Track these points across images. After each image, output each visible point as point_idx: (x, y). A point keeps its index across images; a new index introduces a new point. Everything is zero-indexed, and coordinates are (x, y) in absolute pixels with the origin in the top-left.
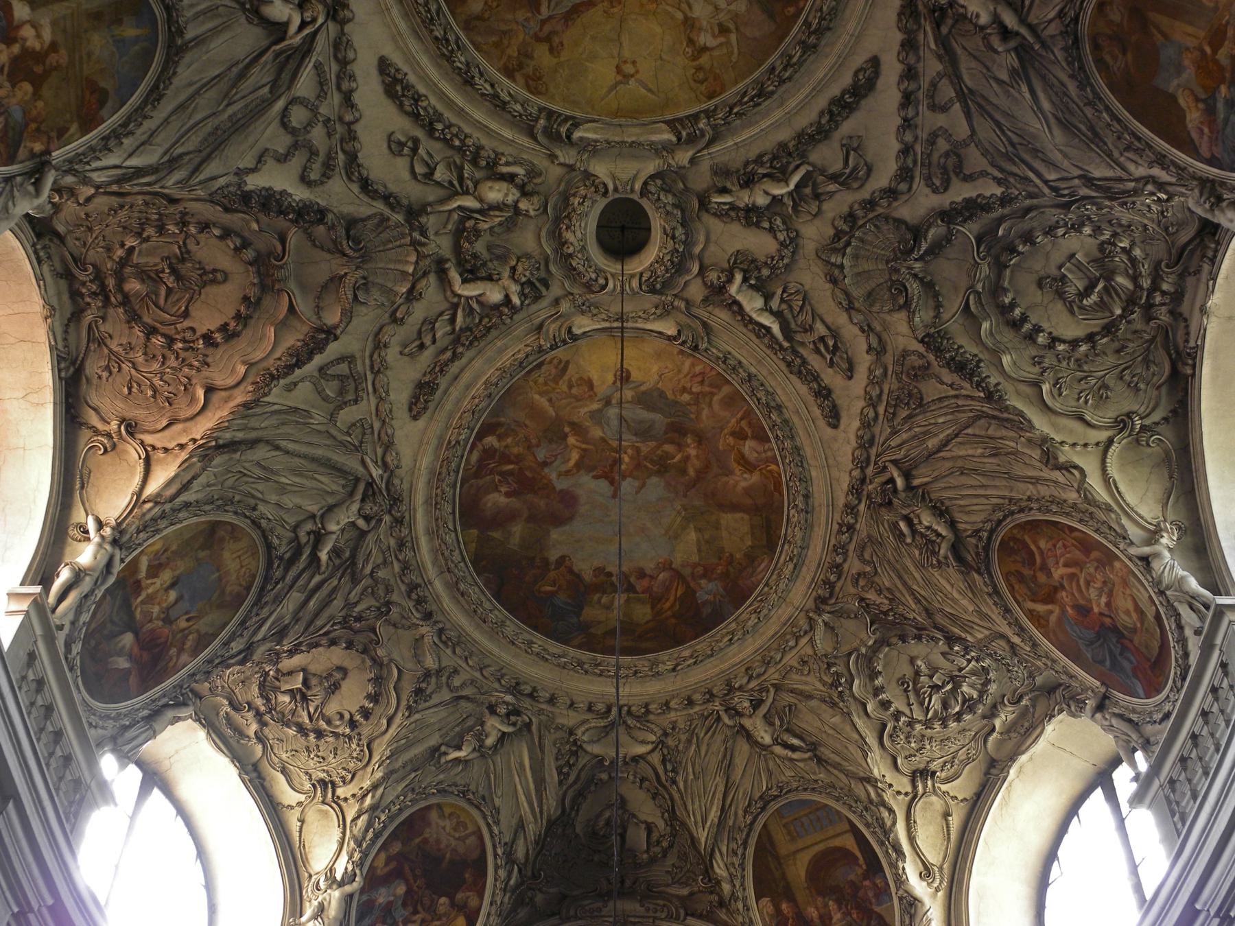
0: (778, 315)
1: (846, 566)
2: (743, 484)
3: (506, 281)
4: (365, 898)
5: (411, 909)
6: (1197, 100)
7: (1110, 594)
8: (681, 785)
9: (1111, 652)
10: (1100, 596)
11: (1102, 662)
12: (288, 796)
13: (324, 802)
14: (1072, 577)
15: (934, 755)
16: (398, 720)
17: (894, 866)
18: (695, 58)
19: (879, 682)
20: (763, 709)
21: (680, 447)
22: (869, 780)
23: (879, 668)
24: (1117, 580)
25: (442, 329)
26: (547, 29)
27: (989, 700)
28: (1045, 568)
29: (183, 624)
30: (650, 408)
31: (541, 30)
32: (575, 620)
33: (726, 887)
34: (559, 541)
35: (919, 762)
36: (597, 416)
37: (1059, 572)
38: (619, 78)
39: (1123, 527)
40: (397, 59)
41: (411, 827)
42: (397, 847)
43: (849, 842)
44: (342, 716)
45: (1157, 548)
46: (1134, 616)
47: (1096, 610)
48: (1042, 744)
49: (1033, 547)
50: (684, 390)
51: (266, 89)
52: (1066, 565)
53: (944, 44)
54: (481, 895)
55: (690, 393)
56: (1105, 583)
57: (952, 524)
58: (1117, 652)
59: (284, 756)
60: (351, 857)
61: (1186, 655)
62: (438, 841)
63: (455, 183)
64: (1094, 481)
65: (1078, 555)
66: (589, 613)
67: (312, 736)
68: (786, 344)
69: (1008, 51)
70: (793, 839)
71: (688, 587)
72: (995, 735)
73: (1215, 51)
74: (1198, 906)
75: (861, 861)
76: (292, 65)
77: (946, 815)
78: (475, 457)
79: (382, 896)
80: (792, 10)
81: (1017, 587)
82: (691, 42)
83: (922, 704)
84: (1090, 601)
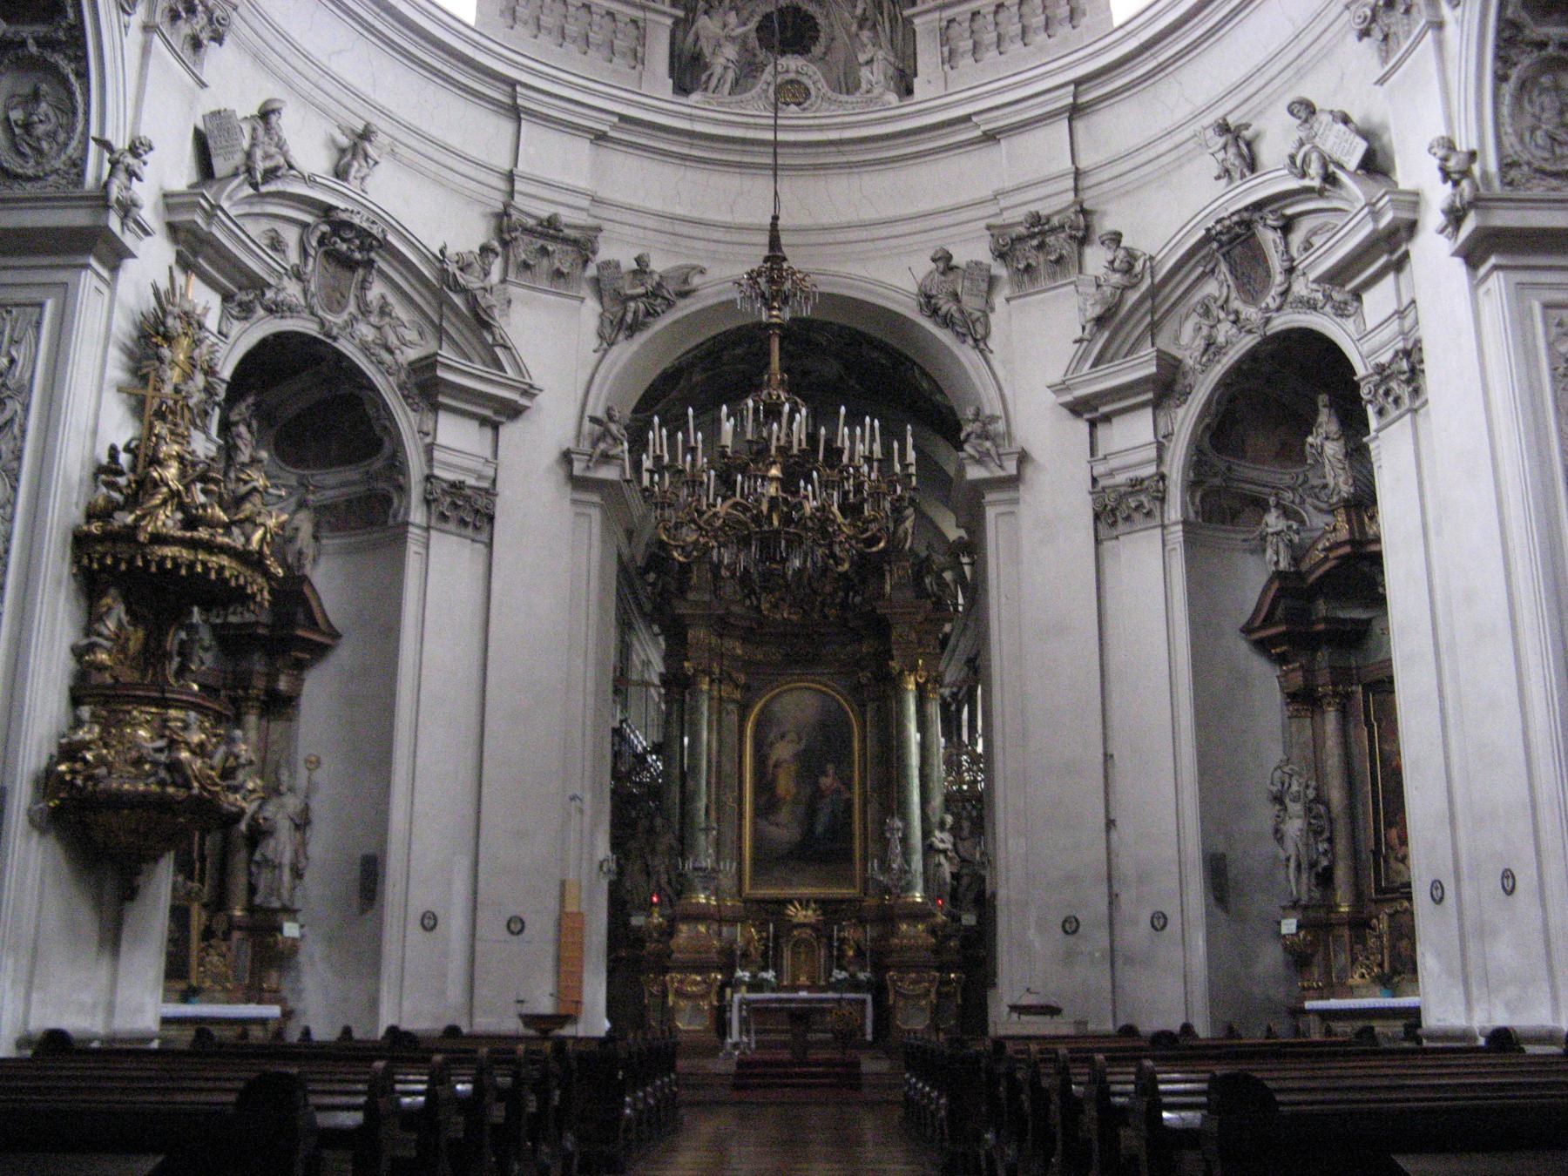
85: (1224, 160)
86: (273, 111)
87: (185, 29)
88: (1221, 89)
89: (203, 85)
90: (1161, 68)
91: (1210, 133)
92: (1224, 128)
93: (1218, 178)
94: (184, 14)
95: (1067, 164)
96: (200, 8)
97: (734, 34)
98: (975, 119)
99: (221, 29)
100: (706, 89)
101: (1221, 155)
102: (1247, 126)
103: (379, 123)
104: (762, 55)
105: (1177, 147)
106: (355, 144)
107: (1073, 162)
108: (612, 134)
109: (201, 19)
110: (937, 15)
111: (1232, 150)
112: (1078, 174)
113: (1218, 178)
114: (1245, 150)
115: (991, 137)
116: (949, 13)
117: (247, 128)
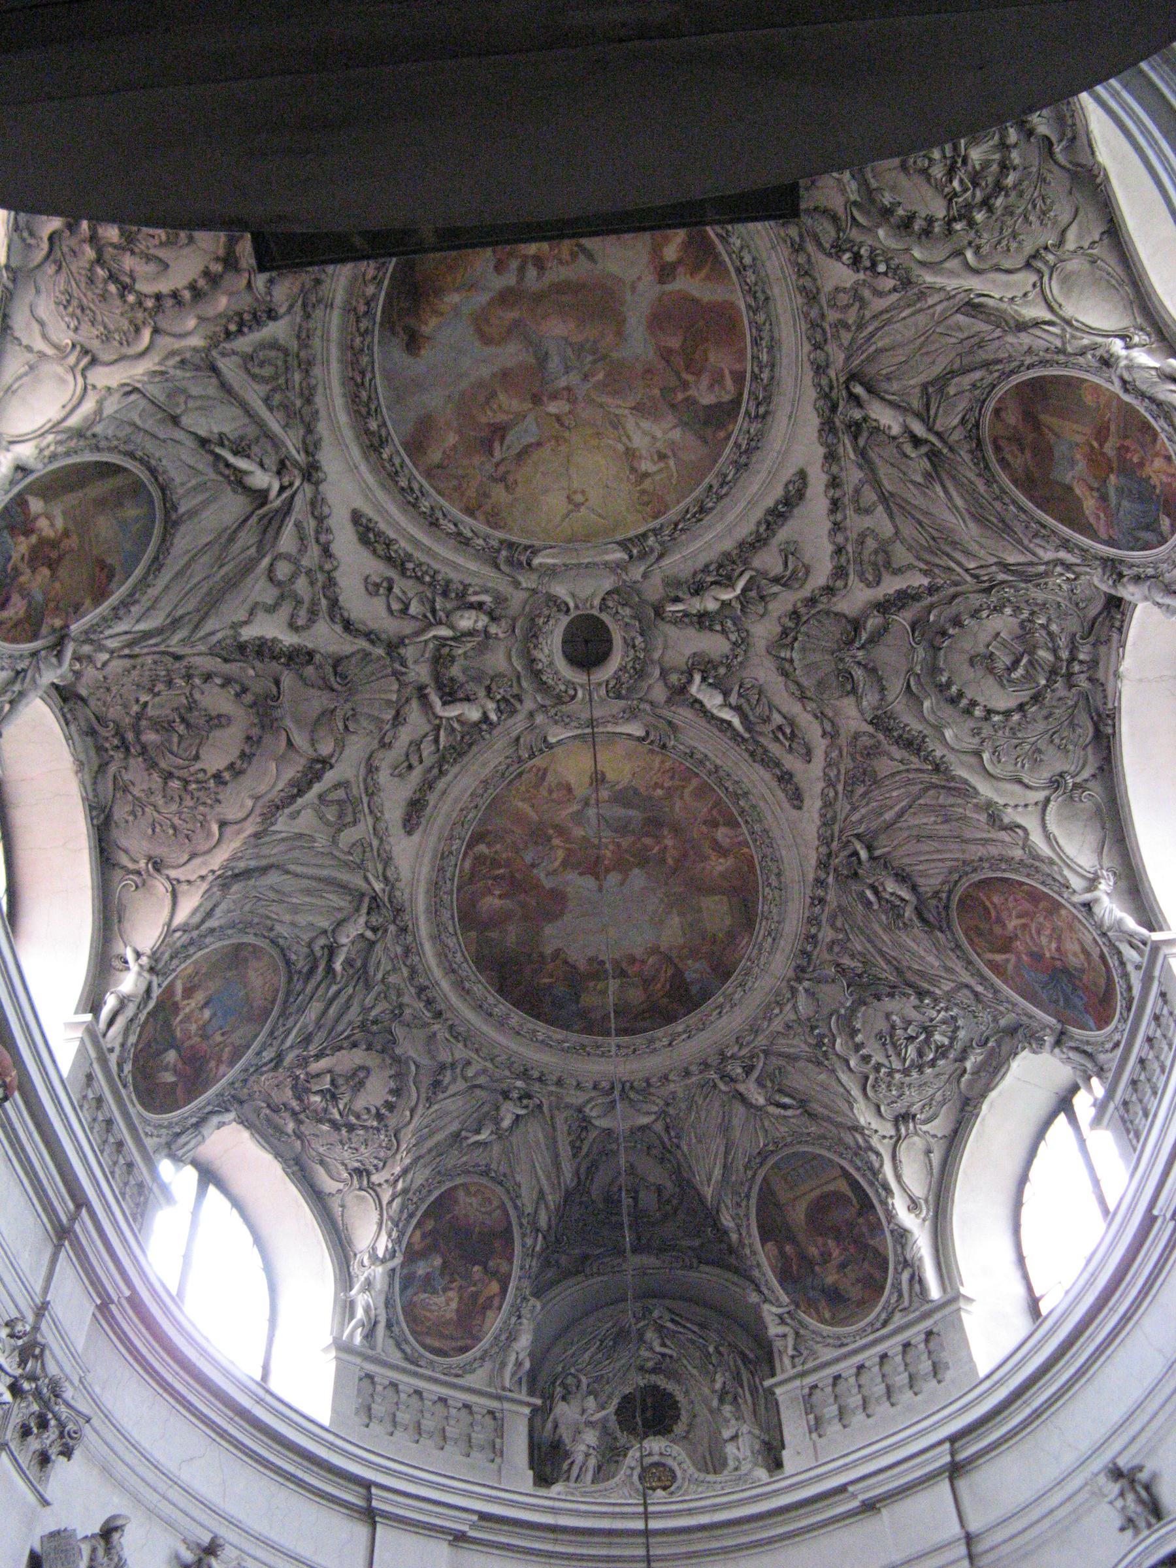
0: (738, 709)
1: (820, 936)
2: (721, 868)
4: (405, 1271)
5: (447, 1278)
6: (1092, 489)
7: (1059, 940)
8: (685, 1148)
9: (1063, 991)
10: (1050, 942)
11: (1056, 1002)
12: (329, 1185)
13: (361, 1189)
14: (1025, 926)
15: (913, 1099)
16: (420, 1111)
17: (884, 1203)
19: (859, 1038)
20: (756, 1074)
21: (658, 839)
22: (856, 1128)
23: (858, 1026)
24: (1065, 926)
25: (427, 749)
26: (502, 469)
27: (958, 1046)
28: (1000, 921)
29: (218, 1038)
30: (628, 805)
32: (574, 1007)
33: (734, 1237)
34: (553, 936)
35: (900, 1107)
36: (578, 818)
37: (1012, 924)
38: (571, 507)
39: (1065, 877)
40: (368, 511)
41: (442, 1205)
42: (430, 1225)
43: (843, 1186)
44: (368, 1110)
45: (1097, 893)
46: (1082, 956)
47: (1048, 955)
48: (1009, 1078)
49: (988, 903)
50: (657, 785)
51: (253, 550)
52: (1019, 917)
53: (862, 453)
54: (510, 1260)
55: (662, 787)
56: (1053, 929)
57: (914, 888)
58: (1069, 990)
59: (321, 1150)
60: (390, 1236)
61: (1129, 988)
62: (466, 1216)
63: (429, 615)
64: (1037, 838)
65: (1027, 906)
66: (587, 1000)
67: (344, 1131)
68: (747, 735)
69: (920, 456)
70: (791, 1188)
71: (676, 966)
72: (966, 1076)
73: (1101, 446)
74: (1155, 1212)
75: (854, 1201)
76: (275, 525)
77: (928, 1152)
78: (468, 864)
79: (421, 1269)
81: (976, 940)
82: (633, 470)
83: (899, 1054)
84: (1042, 948)
85: (1124, 1508)
86: (116, 1529)
87: (34, 1444)
88: (1103, 1431)
89: (45, 1503)
90: (1037, 1414)
91: (1102, 1479)
92: (1117, 1473)
93: (1122, 1529)
94: (35, 1430)
95: (956, 1530)
96: (53, 1422)
97: (593, 1419)
98: (851, 1489)
99: (71, 1443)
100: (568, 1479)
101: (1119, 1503)
102: (1140, 1468)
103: (228, 1534)
104: (623, 1438)
105: (1069, 1499)
106: (200, 1560)
107: (963, 1526)
108: (472, 1534)
109: (52, 1433)
110: (797, 1383)
111: (1130, 1497)
112: (969, 1539)
113: (1122, 1529)
114: (1144, 1494)
115: (870, 1507)
116: (809, 1380)
117: (86, 1549)
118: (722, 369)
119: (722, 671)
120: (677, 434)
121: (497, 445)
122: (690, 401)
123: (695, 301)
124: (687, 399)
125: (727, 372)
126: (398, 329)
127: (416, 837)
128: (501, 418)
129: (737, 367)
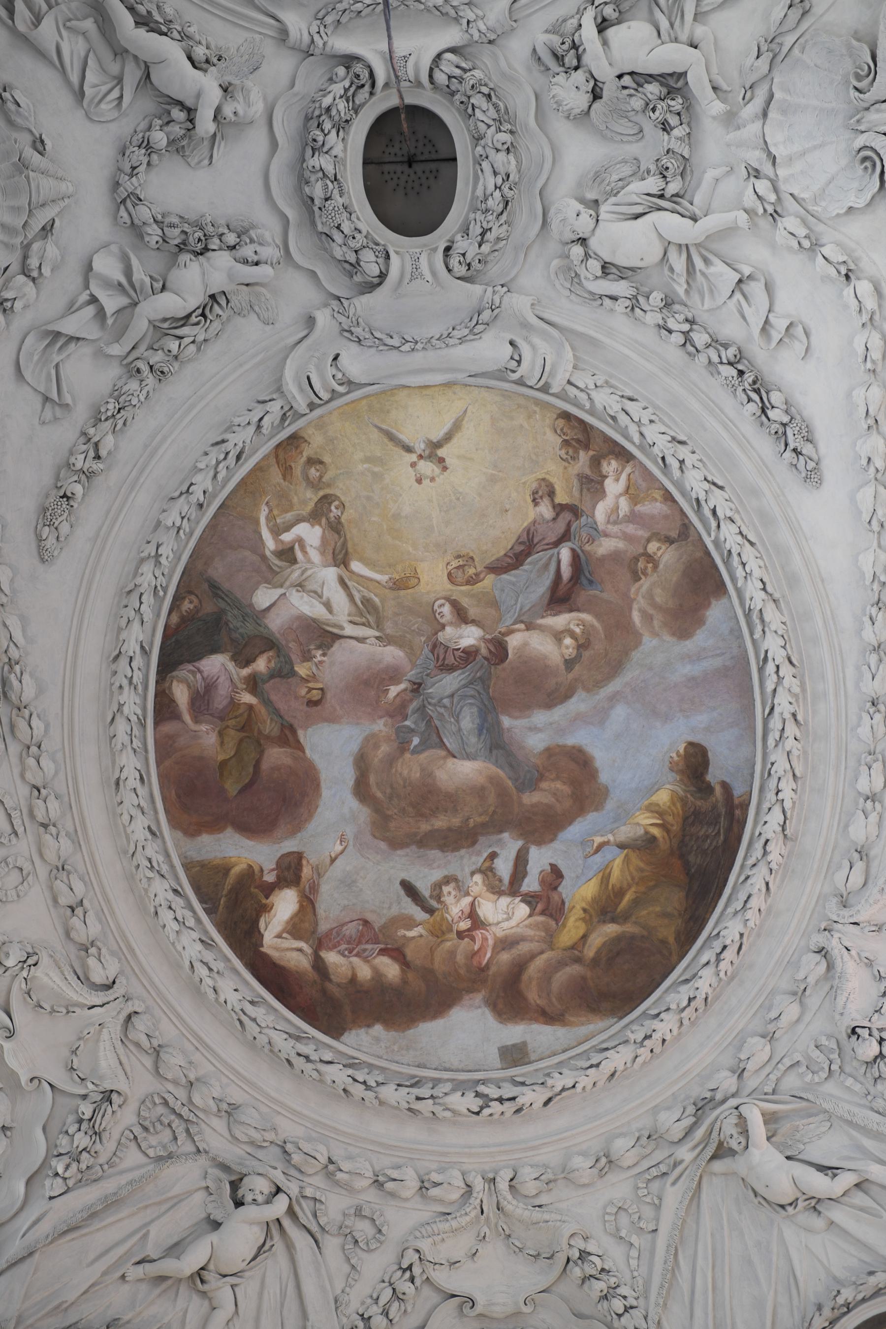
0: (120, 52)
3: (605, 73)
18: (327, 499)
26: (560, 526)
31: (569, 525)
38: (441, 453)
63: (699, 263)
80: (186, 606)
82: (336, 527)
118: (196, 720)
119: (159, 138)
120: (263, 598)
121: (566, 571)
122: (243, 659)
123: (247, 829)
124: (248, 662)
125: (187, 718)
126: (718, 790)
127: (753, 307)
128: (561, 621)
129: (168, 727)
